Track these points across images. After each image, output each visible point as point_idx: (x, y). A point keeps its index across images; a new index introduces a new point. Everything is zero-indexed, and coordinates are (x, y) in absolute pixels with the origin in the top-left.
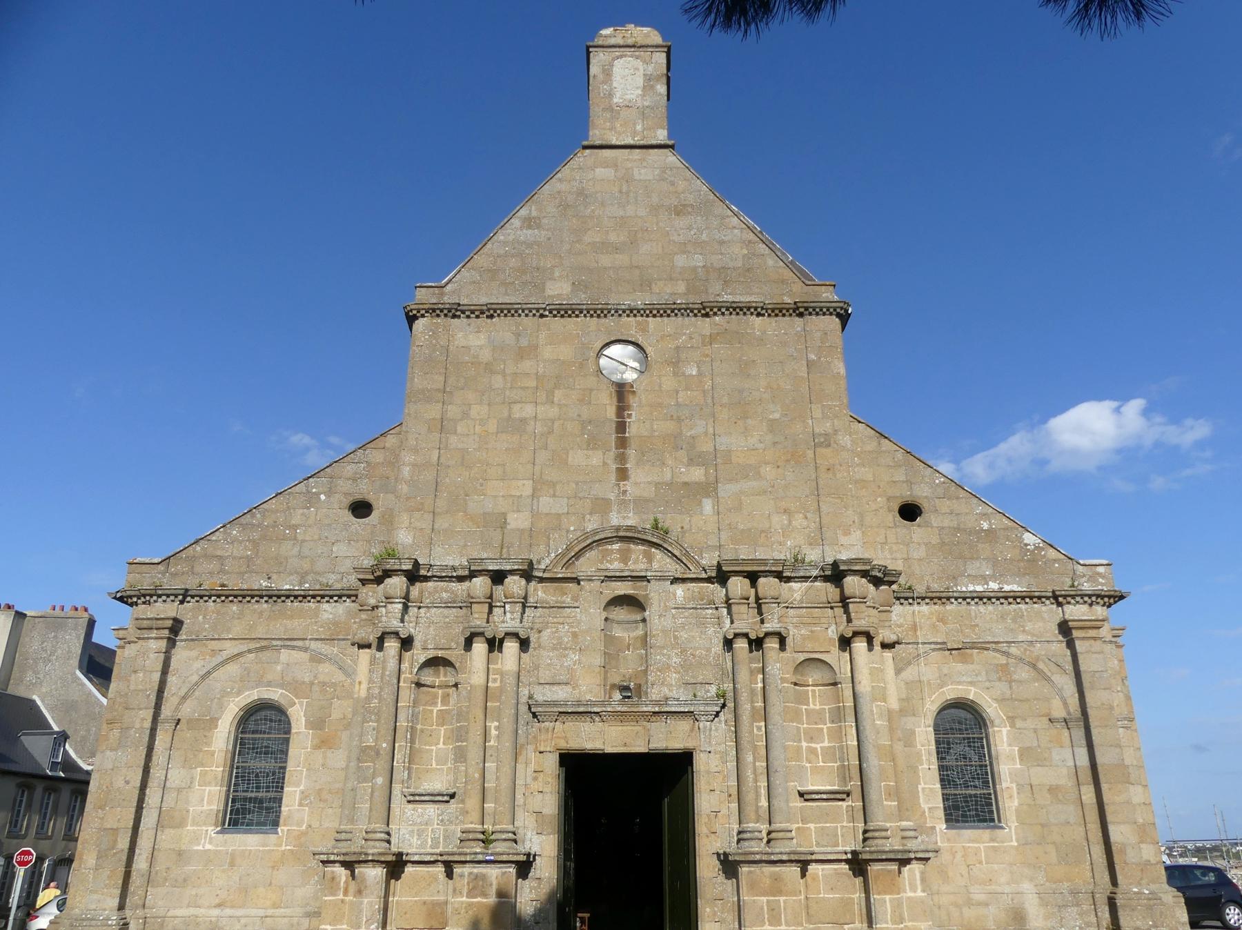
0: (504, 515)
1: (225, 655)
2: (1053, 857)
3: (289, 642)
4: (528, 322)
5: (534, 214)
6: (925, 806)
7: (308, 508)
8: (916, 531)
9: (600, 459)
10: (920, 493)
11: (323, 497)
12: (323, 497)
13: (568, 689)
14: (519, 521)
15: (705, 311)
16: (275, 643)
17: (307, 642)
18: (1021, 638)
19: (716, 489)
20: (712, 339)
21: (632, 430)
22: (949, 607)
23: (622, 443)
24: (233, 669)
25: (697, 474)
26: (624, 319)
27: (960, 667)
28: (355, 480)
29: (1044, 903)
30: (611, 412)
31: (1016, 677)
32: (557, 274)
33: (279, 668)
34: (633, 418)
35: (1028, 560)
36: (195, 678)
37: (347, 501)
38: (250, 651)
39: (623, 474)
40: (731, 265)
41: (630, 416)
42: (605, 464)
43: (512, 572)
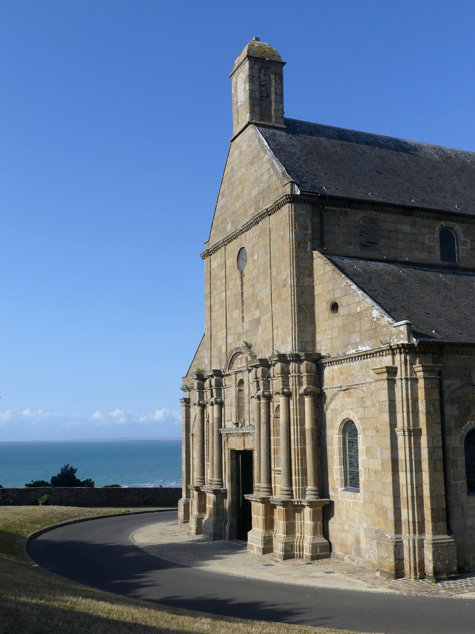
2: (374, 511)
6: (335, 478)
9: (236, 314)
18: (368, 380)
21: (245, 295)
22: (344, 365)
25: (257, 314)
27: (348, 400)
29: (366, 536)
31: (366, 405)
35: (374, 329)
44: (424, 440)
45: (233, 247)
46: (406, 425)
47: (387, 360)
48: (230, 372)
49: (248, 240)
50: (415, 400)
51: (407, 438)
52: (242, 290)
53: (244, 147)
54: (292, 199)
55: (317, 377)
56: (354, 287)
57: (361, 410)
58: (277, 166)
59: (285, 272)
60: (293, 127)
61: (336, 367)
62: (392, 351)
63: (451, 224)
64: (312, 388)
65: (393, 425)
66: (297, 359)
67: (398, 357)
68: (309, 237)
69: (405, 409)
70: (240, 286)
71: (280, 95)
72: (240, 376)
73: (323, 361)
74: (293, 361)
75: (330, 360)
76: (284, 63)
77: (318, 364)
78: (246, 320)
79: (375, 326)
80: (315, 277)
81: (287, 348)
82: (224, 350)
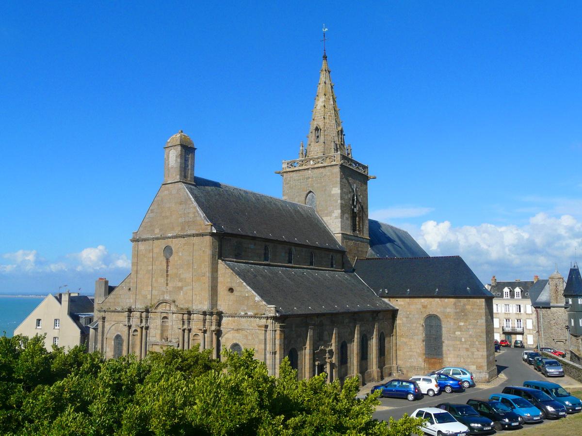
1: (112, 324)
4: (151, 242)
9: (162, 280)
10: (234, 286)
15: (183, 237)
18: (251, 328)
23: (167, 276)
24: (113, 327)
25: (180, 284)
39: (167, 284)
40: (190, 220)
44: (278, 356)
45: (163, 244)
46: (271, 350)
47: (263, 322)
48: (157, 311)
49: (174, 244)
50: (275, 339)
51: (271, 355)
52: (167, 268)
53: (174, 192)
54: (212, 234)
55: (219, 324)
56: (244, 284)
57: (245, 340)
58: (200, 212)
59: (206, 269)
60: (200, 183)
61: (230, 319)
62: (267, 318)
63: (267, 244)
64: (218, 328)
65: (265, 349)
66: (211, 314)
67: (269, 320)
68: (217, 253)
69: (271, 343)
70: (166, 267)
71: (193, 166)
72: (165, 315)
73: (223, 315)
74: (208, 315)
75: (227, 315)
76: (196, 149)
77: (220, 315)
78: (170, 285)
79: (256, 305)
80: (219, 273)
81: (206, 307)
82: (149, 297)
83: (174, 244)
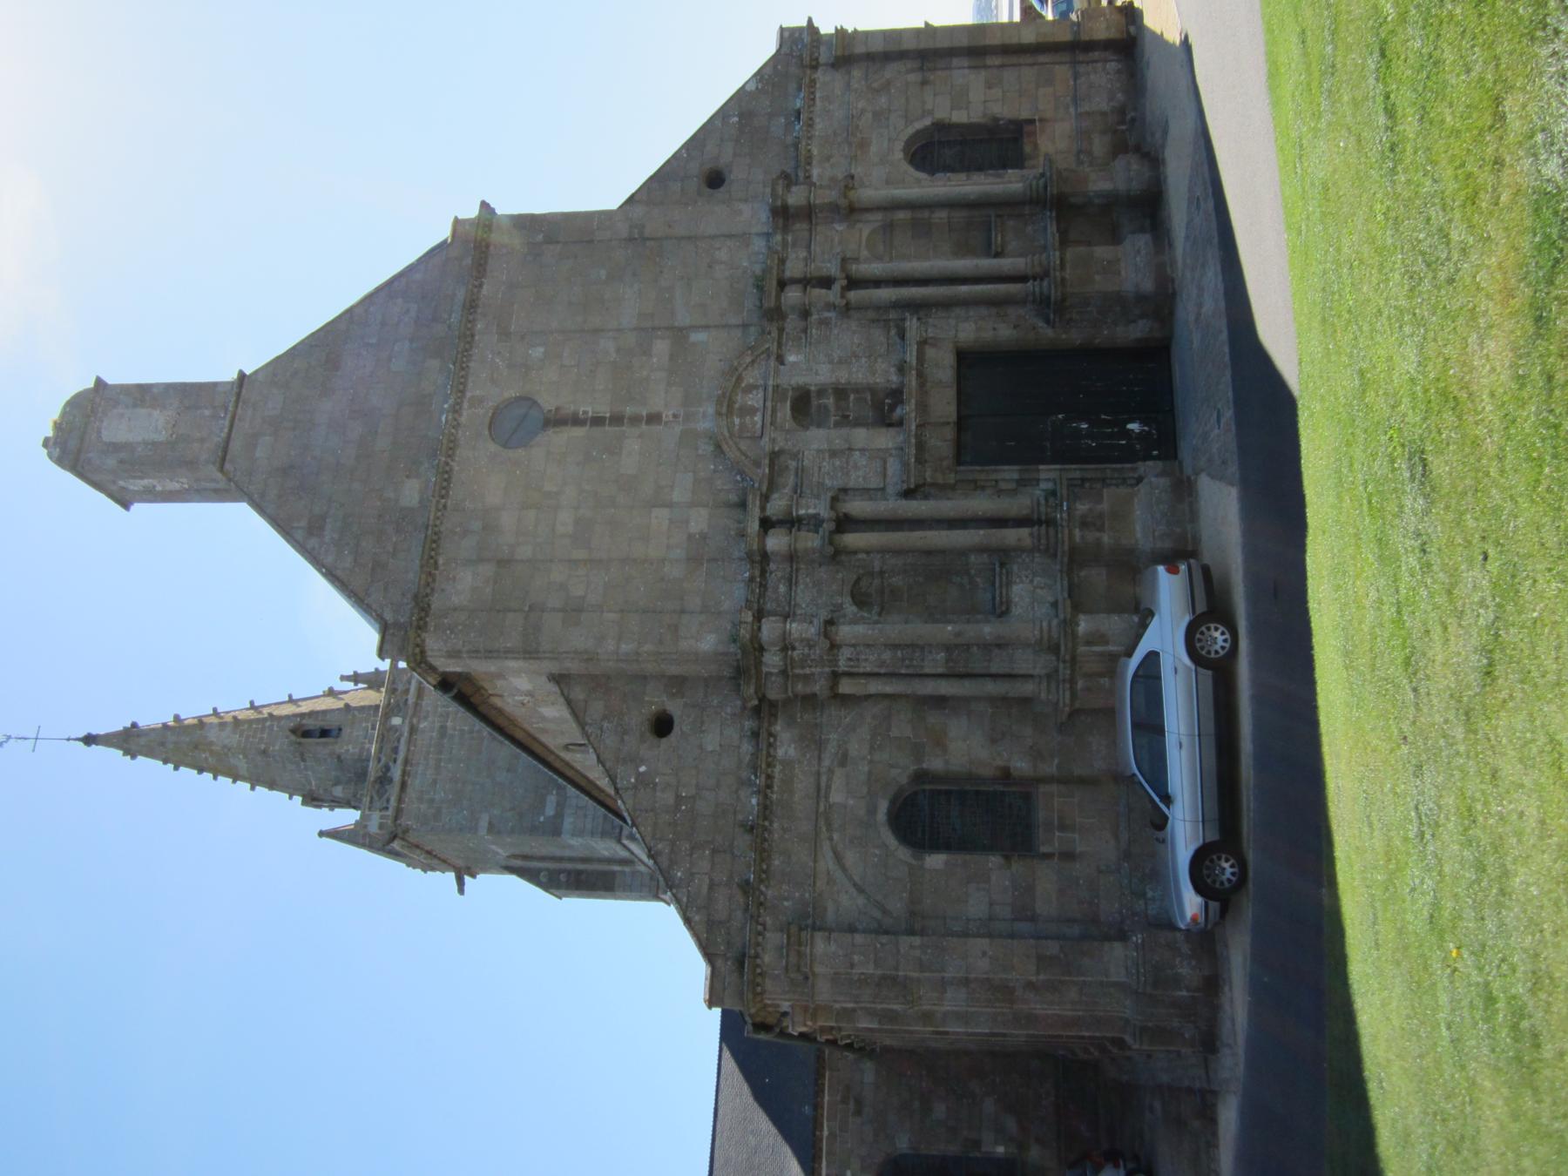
0: (690, 537)
1: (832, 865)
3: (820, 792)
5: (303, 523)
7: (655, 784)
8: (737, 175)
11: (642, 769)
12: (642, 769)
13: (891, 460)
14: (699, 521)
16: (822, 808)
17: (823, 770)
19: (681, 329)
20: (505, 334)
21: (604, 410)
23: (617, 420)
24: (850, 857)
25: (661, 347)
26: (463, 420)
28: (625, 732)
30: (579, 432)
32: (392, 495)
33: (851, 802)
34: (589, 409)
36: (861, 901)
37: (652, 739)
38: (831, 839)
39: (654, 419)
41: (585, 412)
42: (641, 436)
43: (763, 509)
83: (491, 384)
